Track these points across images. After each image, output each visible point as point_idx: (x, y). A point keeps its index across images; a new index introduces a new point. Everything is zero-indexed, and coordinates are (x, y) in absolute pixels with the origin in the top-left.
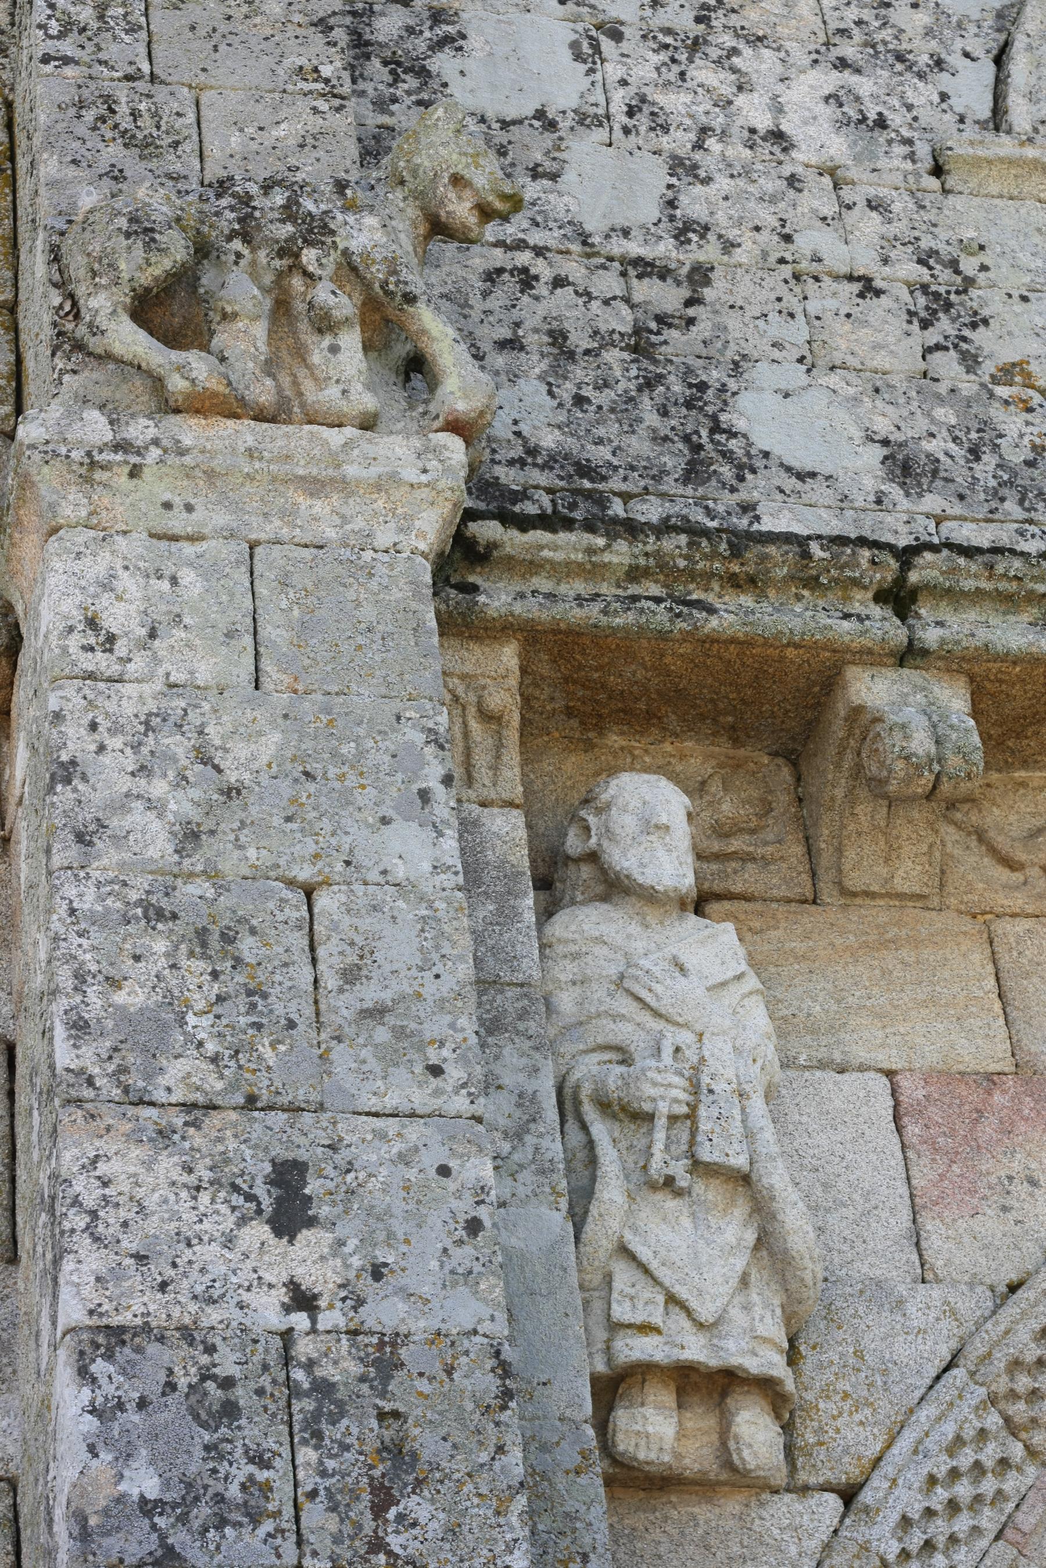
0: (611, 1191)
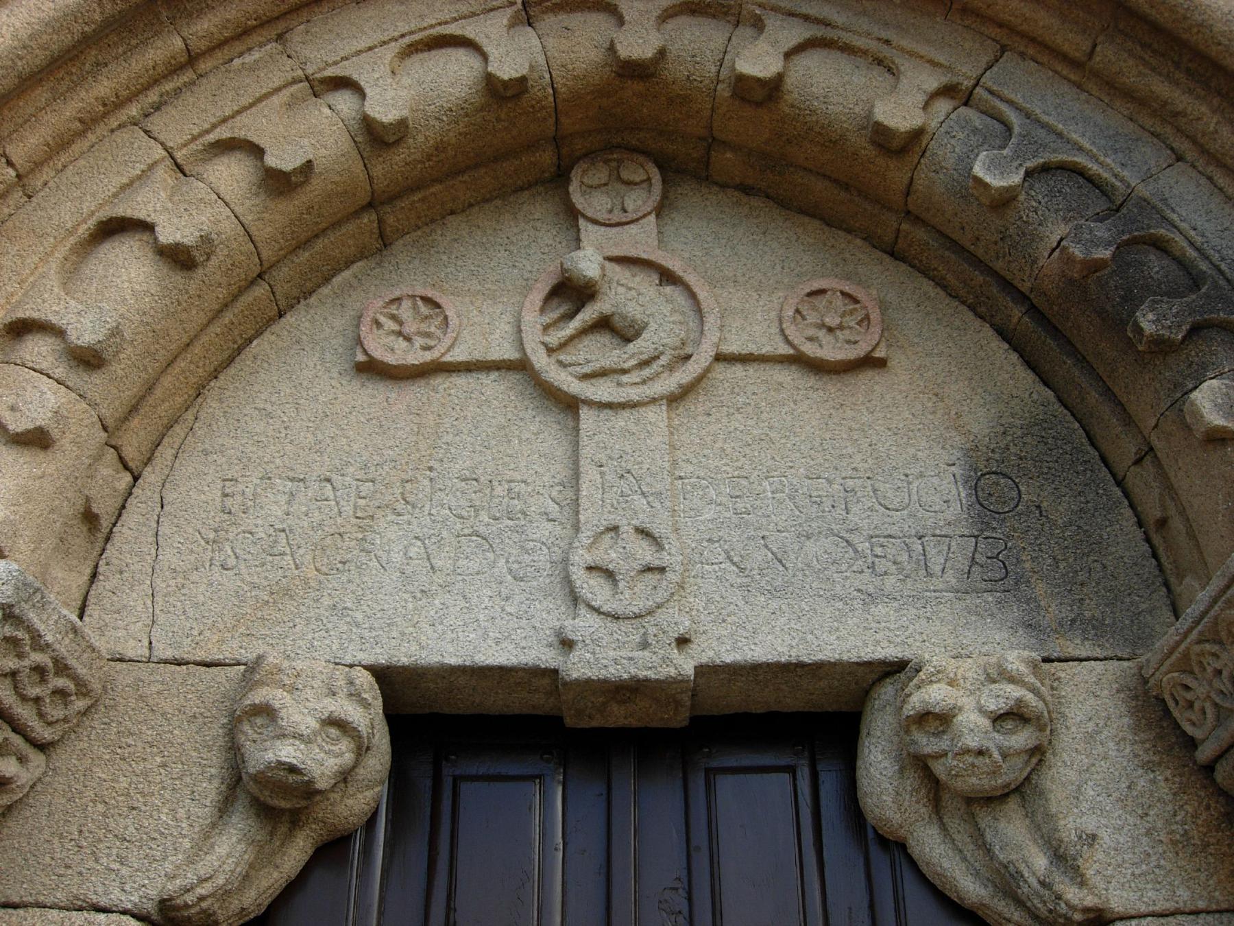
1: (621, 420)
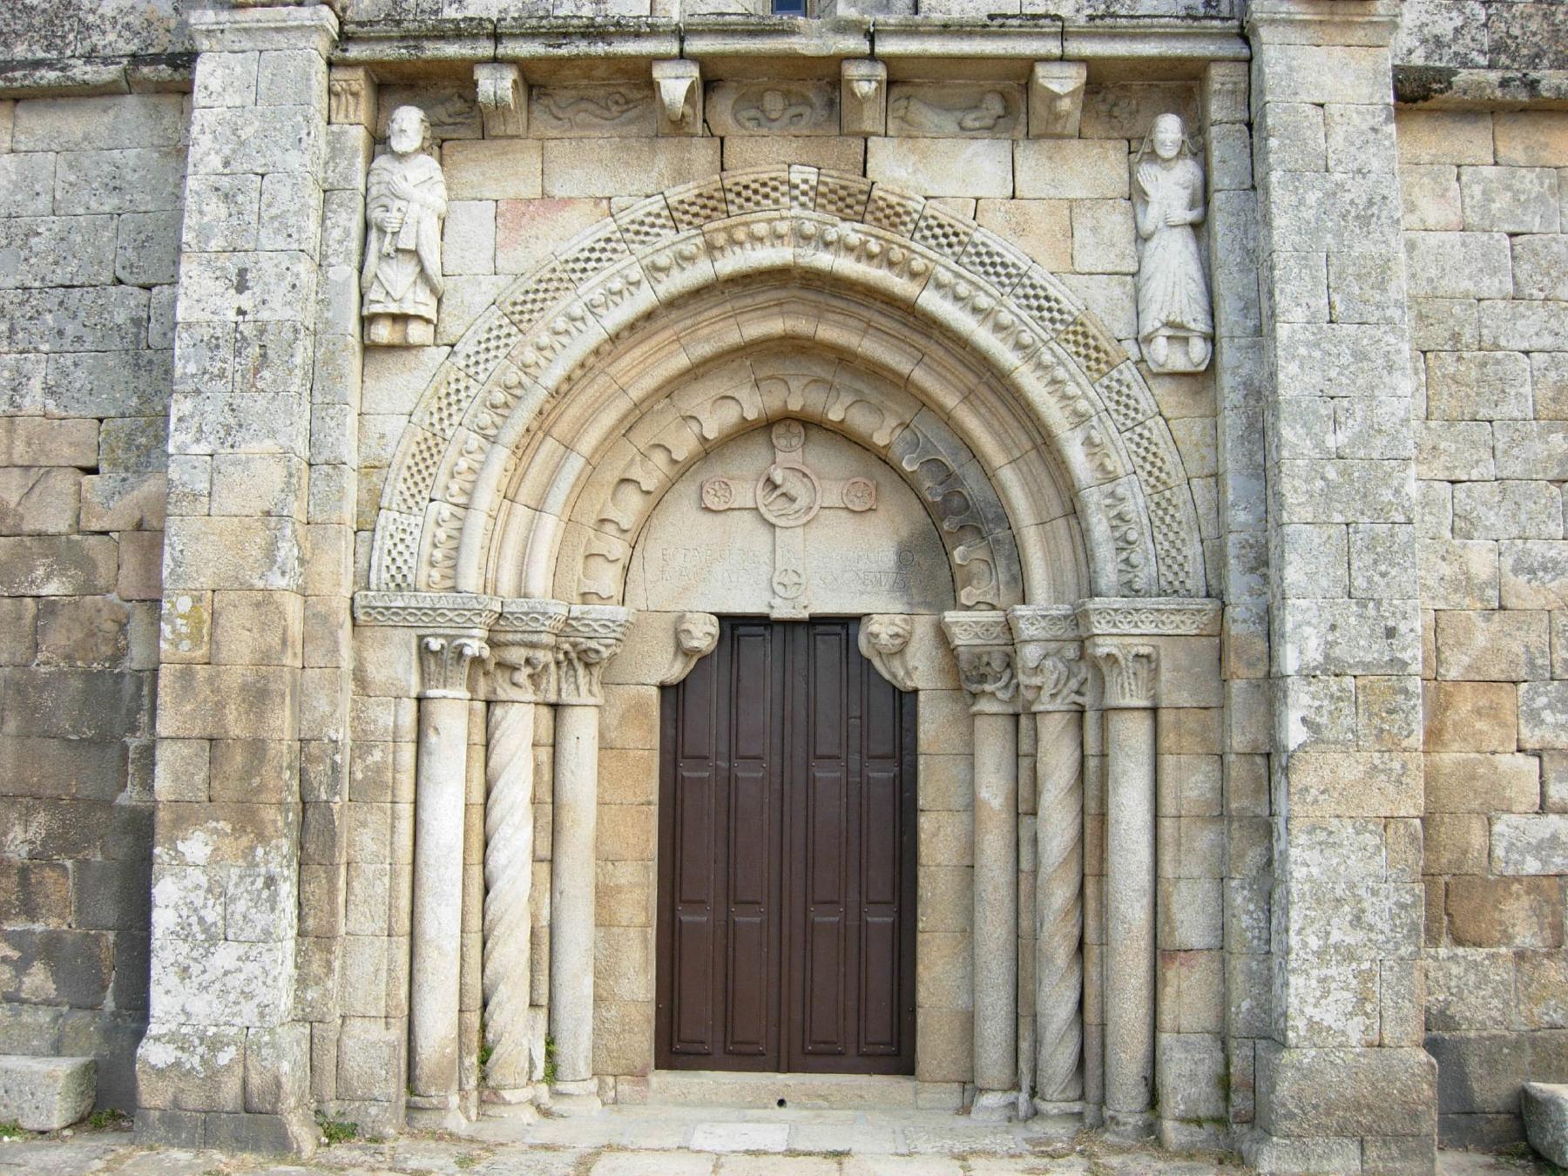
0: (372, 258)
1: (788, 533)
